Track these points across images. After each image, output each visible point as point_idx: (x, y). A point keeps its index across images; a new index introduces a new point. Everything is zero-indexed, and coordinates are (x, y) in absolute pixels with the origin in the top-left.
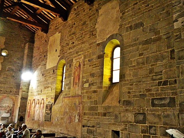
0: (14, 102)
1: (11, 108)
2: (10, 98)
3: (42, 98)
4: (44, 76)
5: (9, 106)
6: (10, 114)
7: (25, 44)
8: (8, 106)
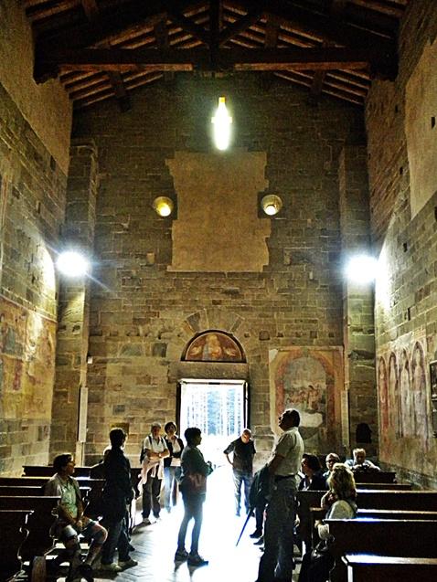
0: (328, 373)
1: (322, 393)
2: (314, 358)
3: (413, 341)
4: (409, 248)
6: (324, 418)
7: (336, 158)
8: (310, 386)
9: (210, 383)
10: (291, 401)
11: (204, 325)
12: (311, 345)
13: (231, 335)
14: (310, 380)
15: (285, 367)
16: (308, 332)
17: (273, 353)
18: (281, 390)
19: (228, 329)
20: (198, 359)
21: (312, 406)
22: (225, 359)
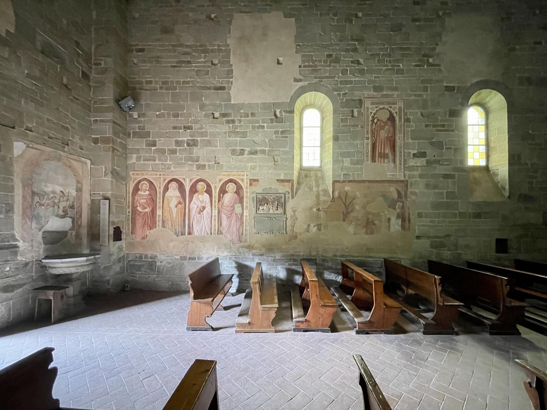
0: (78, 182)
1: (72, 200)
2: (65, 164)
6: (73, 222)
10: (41, 205)
14: (61, 185)
18: (30, 192)
21: (63, 211)
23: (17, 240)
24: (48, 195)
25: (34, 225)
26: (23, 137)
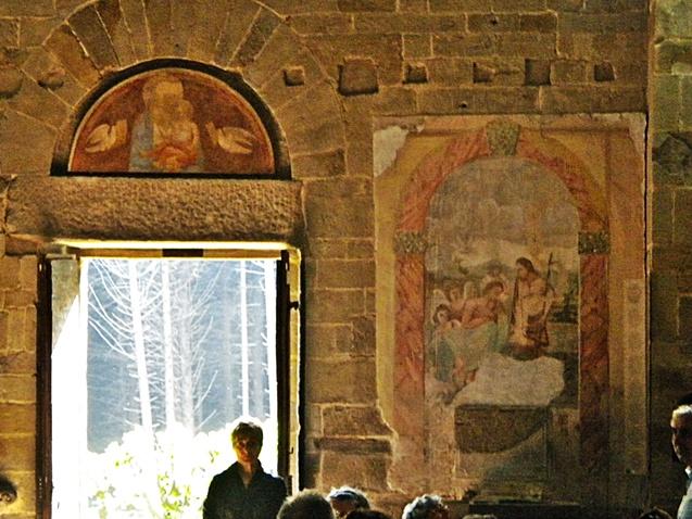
0: (588, 213)
1: (562, 286)
2: (536, 157)
5: (540, 261)
6: (569, 374)
8: (523, 261)
9: (168, 253)
10: (452, 316)
11: (134, 43)
12: (530, 110)
13: (234, 80)
14: (522, 240)
15: (433, 188)
16: (516, 63)
17: (387, 140)
18: (416, 277)
19: (222, 53)
20: (113, 166)
21: (529, 333)
22: (215, 168)
23: (384, 430)
24: (476, 279)
25: (431, 384)
26: (400, 107)
